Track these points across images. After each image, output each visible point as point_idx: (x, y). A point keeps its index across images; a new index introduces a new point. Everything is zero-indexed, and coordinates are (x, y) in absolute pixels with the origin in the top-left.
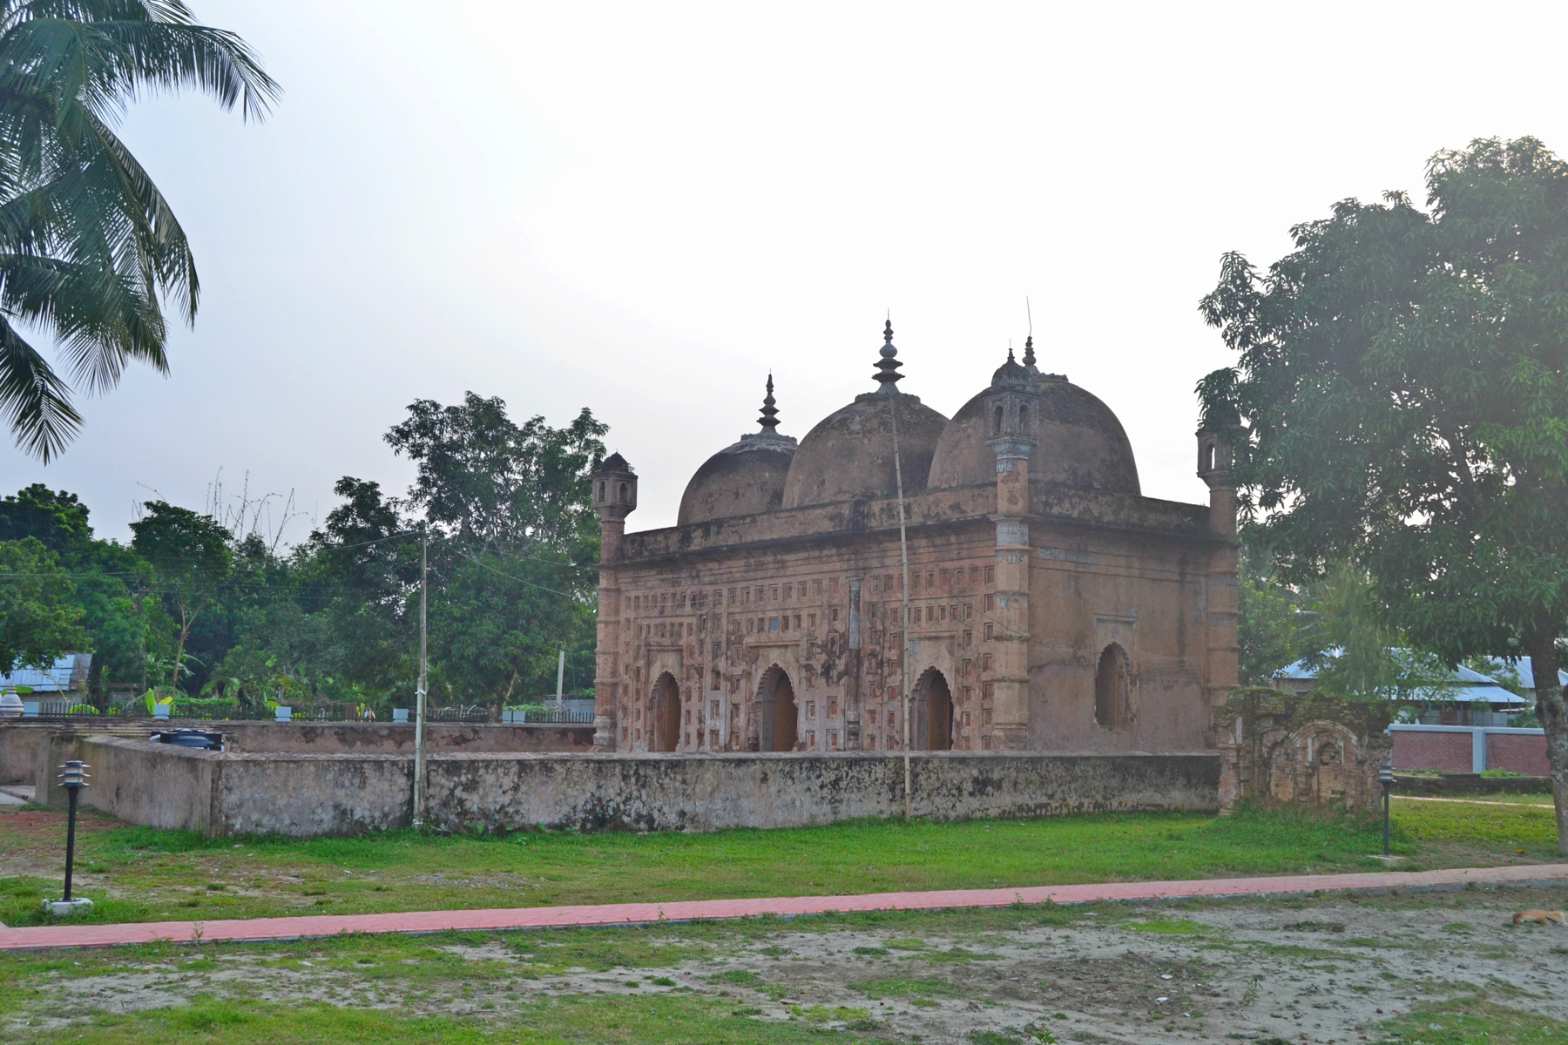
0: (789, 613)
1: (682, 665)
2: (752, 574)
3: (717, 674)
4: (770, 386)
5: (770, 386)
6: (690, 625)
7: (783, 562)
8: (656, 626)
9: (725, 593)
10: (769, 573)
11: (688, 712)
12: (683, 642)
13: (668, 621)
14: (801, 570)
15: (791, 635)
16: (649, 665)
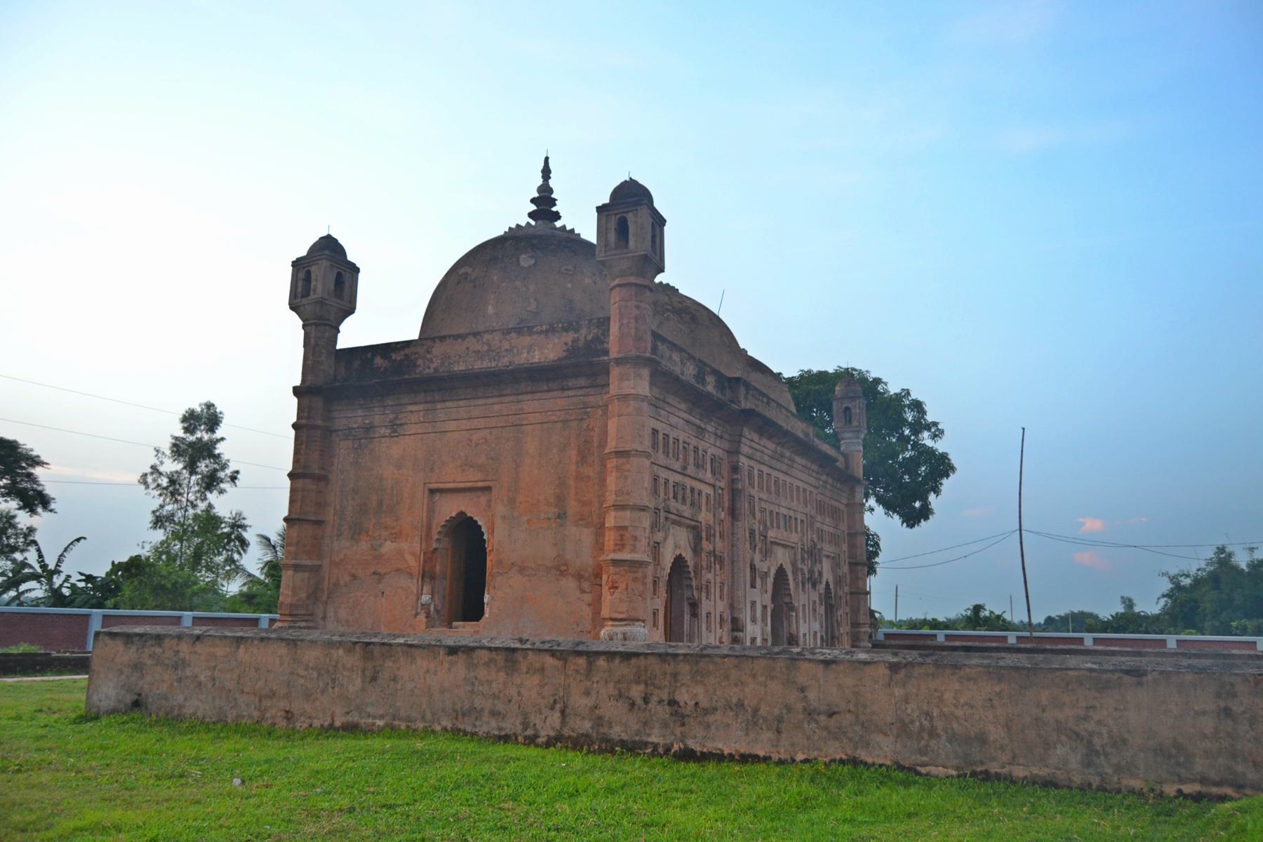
0: (792, 513)
1: (697, 550)
2: (774, 463)
3: (753, 568)
4: (546, 172)
5: (546, 172)
6: (708, 496)
7: (793, 461)
8: (676, 485)
9: (756, 472)
10: (784, 468)
11: (708, 614)
12: (704, 517)
13: (689, 483)
14: (799, 475)
15: (794, 538)
16: (666, 538)
